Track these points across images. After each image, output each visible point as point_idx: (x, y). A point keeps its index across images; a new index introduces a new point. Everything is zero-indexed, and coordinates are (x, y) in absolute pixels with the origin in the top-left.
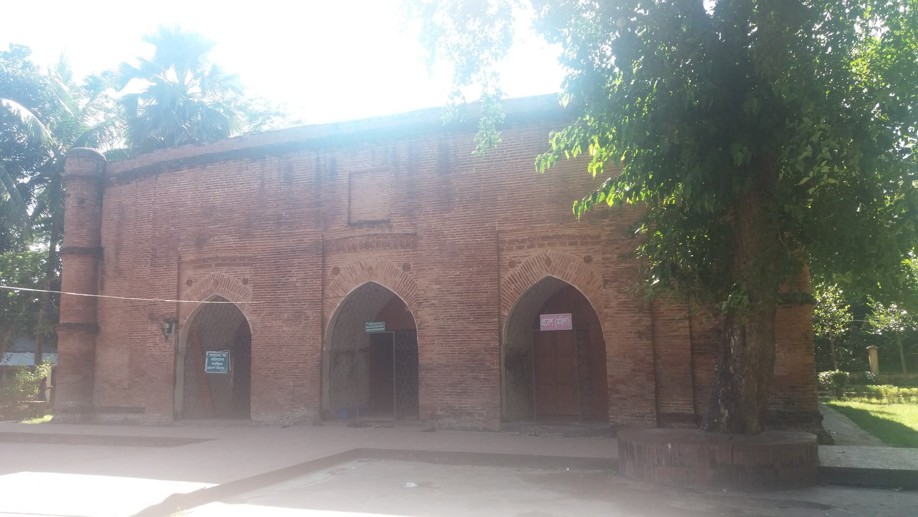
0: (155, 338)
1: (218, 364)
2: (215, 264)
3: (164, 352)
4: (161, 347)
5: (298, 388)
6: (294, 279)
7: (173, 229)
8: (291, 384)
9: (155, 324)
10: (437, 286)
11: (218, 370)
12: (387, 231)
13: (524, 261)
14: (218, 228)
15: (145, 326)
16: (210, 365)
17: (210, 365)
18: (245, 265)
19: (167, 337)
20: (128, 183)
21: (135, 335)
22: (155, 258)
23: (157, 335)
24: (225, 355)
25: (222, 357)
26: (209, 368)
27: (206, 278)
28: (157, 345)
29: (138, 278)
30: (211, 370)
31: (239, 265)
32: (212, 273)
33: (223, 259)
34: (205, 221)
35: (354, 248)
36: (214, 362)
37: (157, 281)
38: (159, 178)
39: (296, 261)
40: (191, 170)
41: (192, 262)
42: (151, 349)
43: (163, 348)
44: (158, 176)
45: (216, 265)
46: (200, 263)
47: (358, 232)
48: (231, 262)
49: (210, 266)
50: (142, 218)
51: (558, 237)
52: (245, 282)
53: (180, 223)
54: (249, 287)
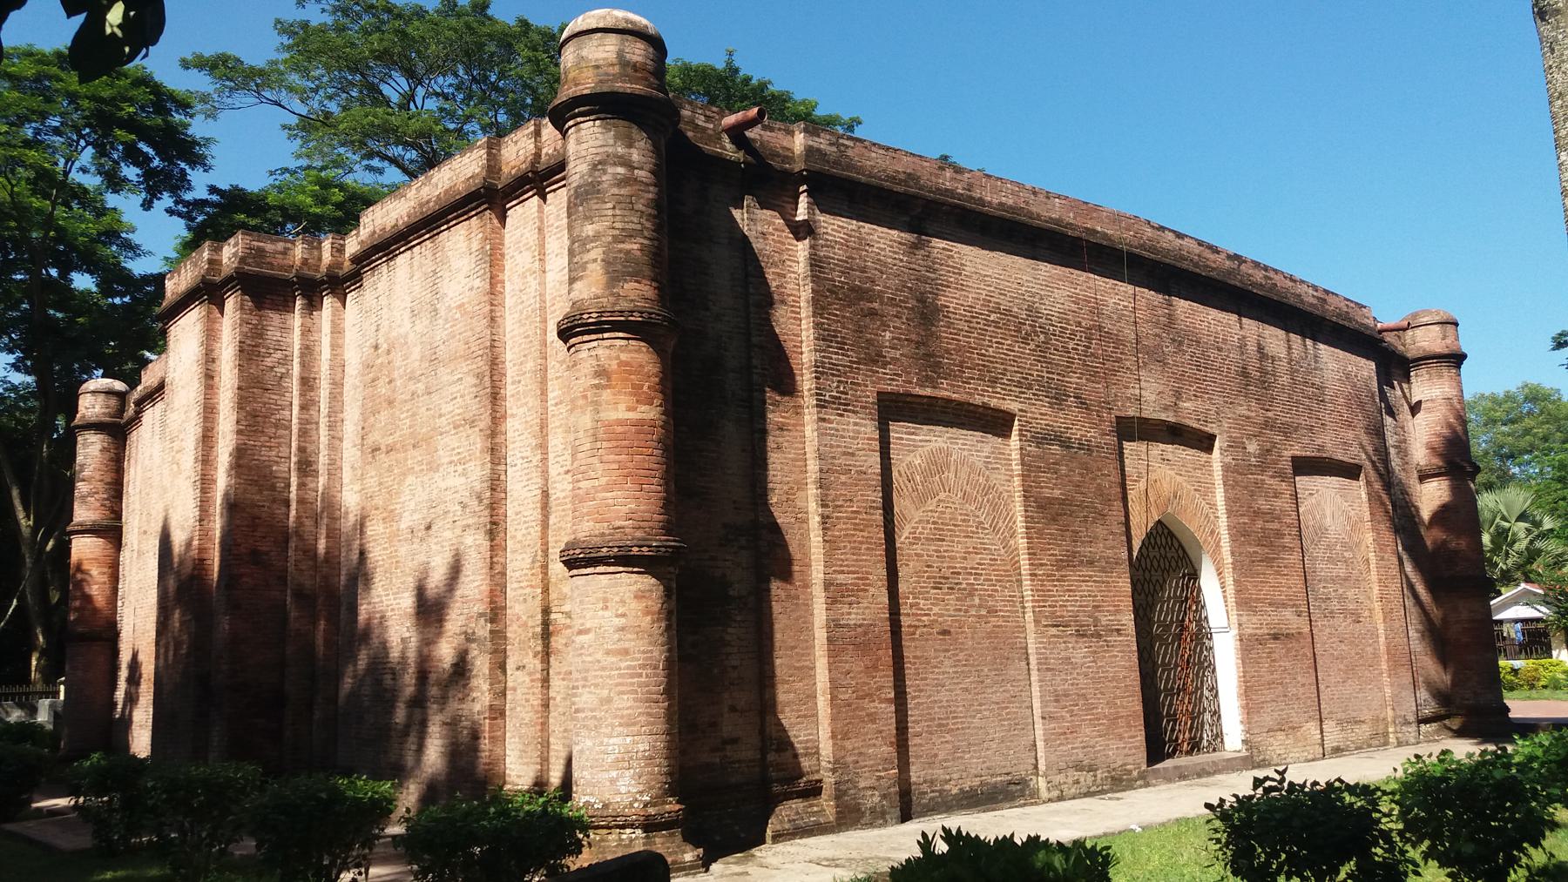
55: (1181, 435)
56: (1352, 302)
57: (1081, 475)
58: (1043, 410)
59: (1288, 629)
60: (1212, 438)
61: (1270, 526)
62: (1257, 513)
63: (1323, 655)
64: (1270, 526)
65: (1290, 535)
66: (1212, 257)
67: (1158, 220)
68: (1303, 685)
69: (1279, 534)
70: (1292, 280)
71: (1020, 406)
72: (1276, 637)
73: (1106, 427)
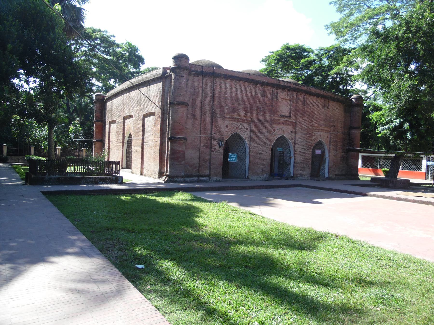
1: (233, 158)
6: (264, 131)
8: (262, 166)
10: (300, 139)
11: (233, 161)
12: (289, 120)
13: (316, 135)
16: (230, 158)
17: (230, 158)
18: (247, 123)
19: (220, 147)
20: (198, 76)
23: (216, 146)
25: (235, 156)
26: (230, 160)
27: (233, 125)
30: (231, 161)
31: (245, 122)
32: (235, 124)
33: (241, 119)
34: (236, 103)
35: (280, 123)
38: (217, 80)
39: (265, 125)
41: (229, 118)
45: (237, 121)
46: (232, 119)
47: (282, 118)
48: (242, 121)
49: (235, 121)
51: (324, 130)
52: (247, 129)
54: (248, 132)
61: (138, 130)
62: (137, 128)
72: (136, 151)
73: (122, 119)
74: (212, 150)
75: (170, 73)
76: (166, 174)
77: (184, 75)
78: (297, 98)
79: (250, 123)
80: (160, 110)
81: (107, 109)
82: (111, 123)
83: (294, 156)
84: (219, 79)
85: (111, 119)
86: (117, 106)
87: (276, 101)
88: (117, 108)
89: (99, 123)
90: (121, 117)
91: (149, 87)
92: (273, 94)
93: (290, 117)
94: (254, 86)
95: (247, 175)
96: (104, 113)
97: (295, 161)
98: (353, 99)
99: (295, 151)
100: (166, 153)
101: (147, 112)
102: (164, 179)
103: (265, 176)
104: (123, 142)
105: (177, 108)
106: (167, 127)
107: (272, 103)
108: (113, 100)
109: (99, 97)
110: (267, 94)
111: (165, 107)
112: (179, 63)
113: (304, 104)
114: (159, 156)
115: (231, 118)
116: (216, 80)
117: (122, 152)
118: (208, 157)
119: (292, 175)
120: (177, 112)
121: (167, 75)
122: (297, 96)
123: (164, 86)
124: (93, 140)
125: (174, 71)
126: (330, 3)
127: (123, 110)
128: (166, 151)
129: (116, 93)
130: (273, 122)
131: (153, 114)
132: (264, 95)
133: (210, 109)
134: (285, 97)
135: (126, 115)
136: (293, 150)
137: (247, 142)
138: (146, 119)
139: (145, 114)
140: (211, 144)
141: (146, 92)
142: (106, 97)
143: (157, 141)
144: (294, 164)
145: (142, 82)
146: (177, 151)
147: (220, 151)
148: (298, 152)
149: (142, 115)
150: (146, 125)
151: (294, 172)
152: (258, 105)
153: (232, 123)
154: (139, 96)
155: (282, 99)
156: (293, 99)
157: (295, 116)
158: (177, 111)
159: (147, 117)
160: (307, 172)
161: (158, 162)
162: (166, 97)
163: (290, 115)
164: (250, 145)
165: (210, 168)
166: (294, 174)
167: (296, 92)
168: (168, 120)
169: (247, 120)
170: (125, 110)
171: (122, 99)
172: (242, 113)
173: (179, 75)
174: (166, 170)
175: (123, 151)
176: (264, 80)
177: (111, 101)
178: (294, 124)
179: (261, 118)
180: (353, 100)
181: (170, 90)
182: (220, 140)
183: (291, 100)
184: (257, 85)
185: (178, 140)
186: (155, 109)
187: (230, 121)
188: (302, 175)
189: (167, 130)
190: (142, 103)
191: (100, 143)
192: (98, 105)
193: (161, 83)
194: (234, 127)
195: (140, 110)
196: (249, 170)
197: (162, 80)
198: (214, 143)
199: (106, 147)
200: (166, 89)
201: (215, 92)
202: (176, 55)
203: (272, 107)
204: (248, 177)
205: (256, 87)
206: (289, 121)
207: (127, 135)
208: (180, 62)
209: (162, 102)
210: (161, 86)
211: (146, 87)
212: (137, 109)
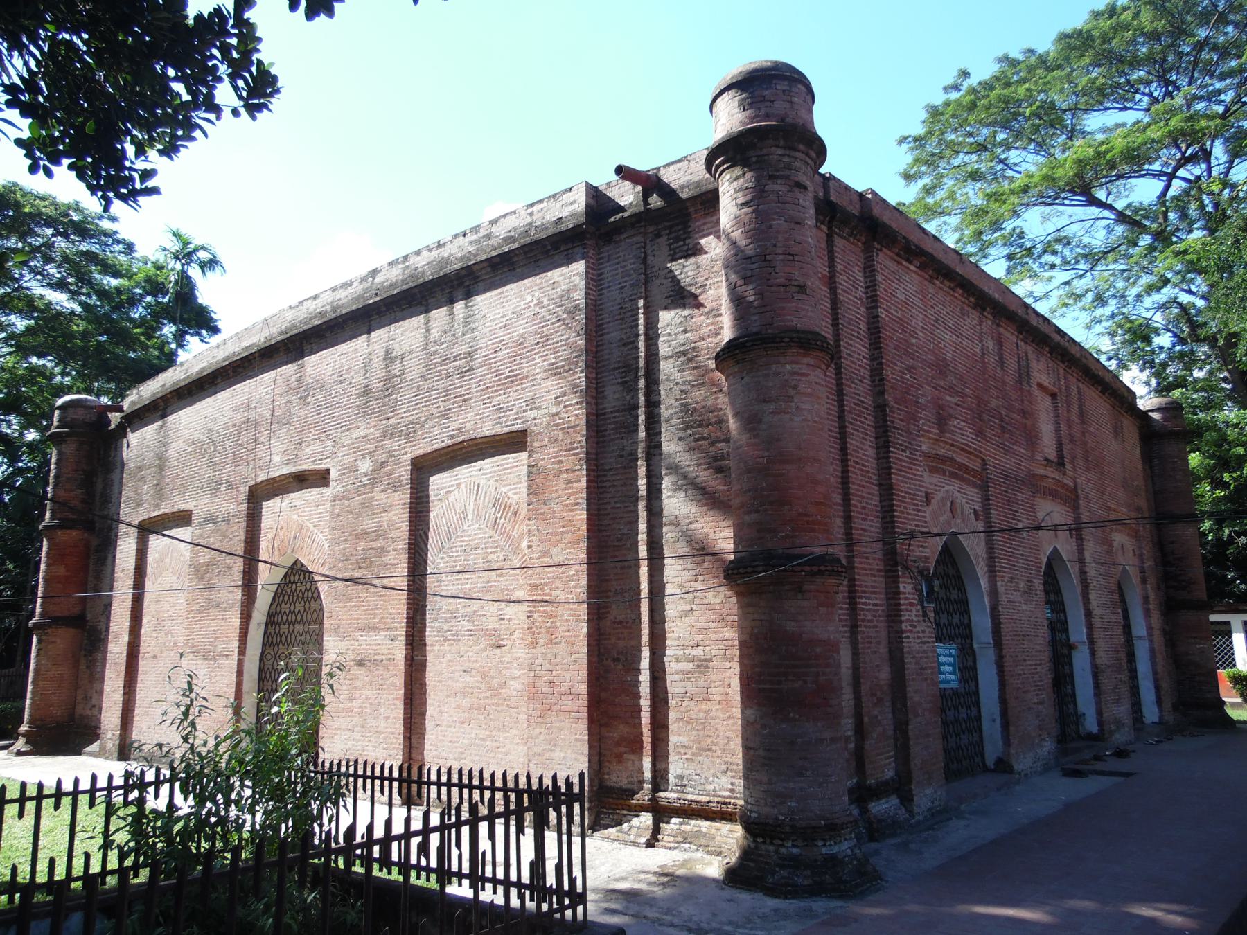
0: (911, 611)
2: (949, 471)
3: (924, 643)
4: (918, 632)
5: (1040, 707)
7: (908, 376)
8: (1036, 701)
9: (907, 577)
11: (948, 682)
14: (956, 404)
15: (875, 581)
18: (974, 485)
19: (925, 614)
21: (864, 600)
22: (895, 428)
24: (953, 651)
25: (950, 655)
28: (915, 627)
29: (857, 463)
32: (947, 487)
33: (961, 466)
34: (942, 383)
36: (943, 664)
37: (902, 481)
38: (881, 255)
39: (1021, 496)
40: (920, 272)
42: (908, 637)
43: (921, 635)
44: (881, 250)
45: (954, 475)
46: (938, 464)
48: (960, 473)
50: (850, 324)
53: (914, 368)
55: (307, 480)
56: (541, 201)
57: (221, 541)
58: (208, 501)
59: (378, 654)
60: (328, 471)
61: (374, 545)
63: (435, 686)
64: (374, 545)
65: (394, 550)
66: (351, 290)
67: (294, 302)
68: (387, 718)
69: (383, 551)
70: (440, 245)
71: (194, 503)
72: (360, 663)
73: (242, 497)
74: (904, 626)
75: (646, 203)
76: (653, 799)
77: (808, 183)
78: (1067, 388)
79: (981, 488)
80: (577, 414)
81: (131, 466)
82: (147, 529)
83: (1091, 641)
84: (888, 252)
85: (157, 506)
86: (203, 438)
87: (1029, 391)
88: (205, 449)
89: (74, 533)
90: (230, 486)
91: (459, 306)
92: (1019, 362)
93: (1063, 465)
94: (975, 314)
95: (992, 752)
96: (99, 486)
97: (1098, 661)
98: (1151, 414)
99: (1089, 614)
100: (645, 664)
101: (452, 437)
102: (648, 834)
103: (1048, 746)
104: (246, 617)
105: (788, 367)
106: (642, 505)
107: (1022, 401)
108: (171, 418)
109: (81, 411)
110: (1006, 355)
111: (613, 396)
112: (780, 106)
113: (1082, 414)
114: (591, 694)
115: (936, 457)
116: (877, 255)
117: (240, 673)
118: (884, 675)
119: (1094, 729)
120: (791, 392)
121: (626, 214)
122: (1065, 378)
123: (594, 281)
124: (34, 621)
125: (751, 153)
126: (902, 140)
127: (245, 452)
128: (646, 653)
129: (194, 378)
130: (1034, 484)
131: (515, 442)
132: (1001, 361)
133: (868, 401)
134: (1046, 380)
135: (273, 475)
136: (1083, 612)
137: (984, 583)
138: (432, 479)
139: (429, 449)
140: (893, 596)
141: (435, 333)
142: (120, 409)
143: (557, 594)
144: (1095, 676)
145: (404, 287)
146: (818, 650)
147: (927, 630)
148: (1097, 622)
149: (409, 457)
150: (436, 513)
151: (1099, 713)
152: (994, 403)
153: (935, 481)
154: (378, 363)
155: (1040, 385)
156: (1060, 389)
157: (1074, 458)
158: (795, 387)
159: (442, 470)
160: (1122, 711)
161: (583, 725)
162: (614, 334)
163: (1061, 457)
164: (994, 593)
165: (906, 738)
166: (1100, 723)
167: (1063, 362)
168: (640, 462)
169: (974, 473)
170: (261, 451)
171: (238, 401)
172: (963, 432)
173: (787, 177)
174: (648, 775)
175: (240, 663)
176: (996, 296)
177: (160, 423)
178: (1071, 497)
179: (1008, 463)
180: (1156, 416)
181: (646, 299)
182: (921, 573)
183: (1053, 396)
184: (984, 309)
185: (821, 573)
186: (532, 414)
187: (933, 470)
188: (1119, 724)
189: (643, 526)
190: (405, 394)
191: (72, 631)
192: (70, 449)
193: (580, 266)
194: (944, 505)
195: (387, 434)
196: (1006, 725)
197: (584, 246)
198: (906, 587)
199: (117, 647)
200: (613, 296)
201: (882, 312)
202: (753, 66)
203: (1027, 419)
204: (999, 761)
205: (980, 323)
206: (1063, 485)
207: (267, 577)
208: (788, 105)
209: (587, 367)
210: (580, 283)
211: (439, 316)
212: (356, 433)
